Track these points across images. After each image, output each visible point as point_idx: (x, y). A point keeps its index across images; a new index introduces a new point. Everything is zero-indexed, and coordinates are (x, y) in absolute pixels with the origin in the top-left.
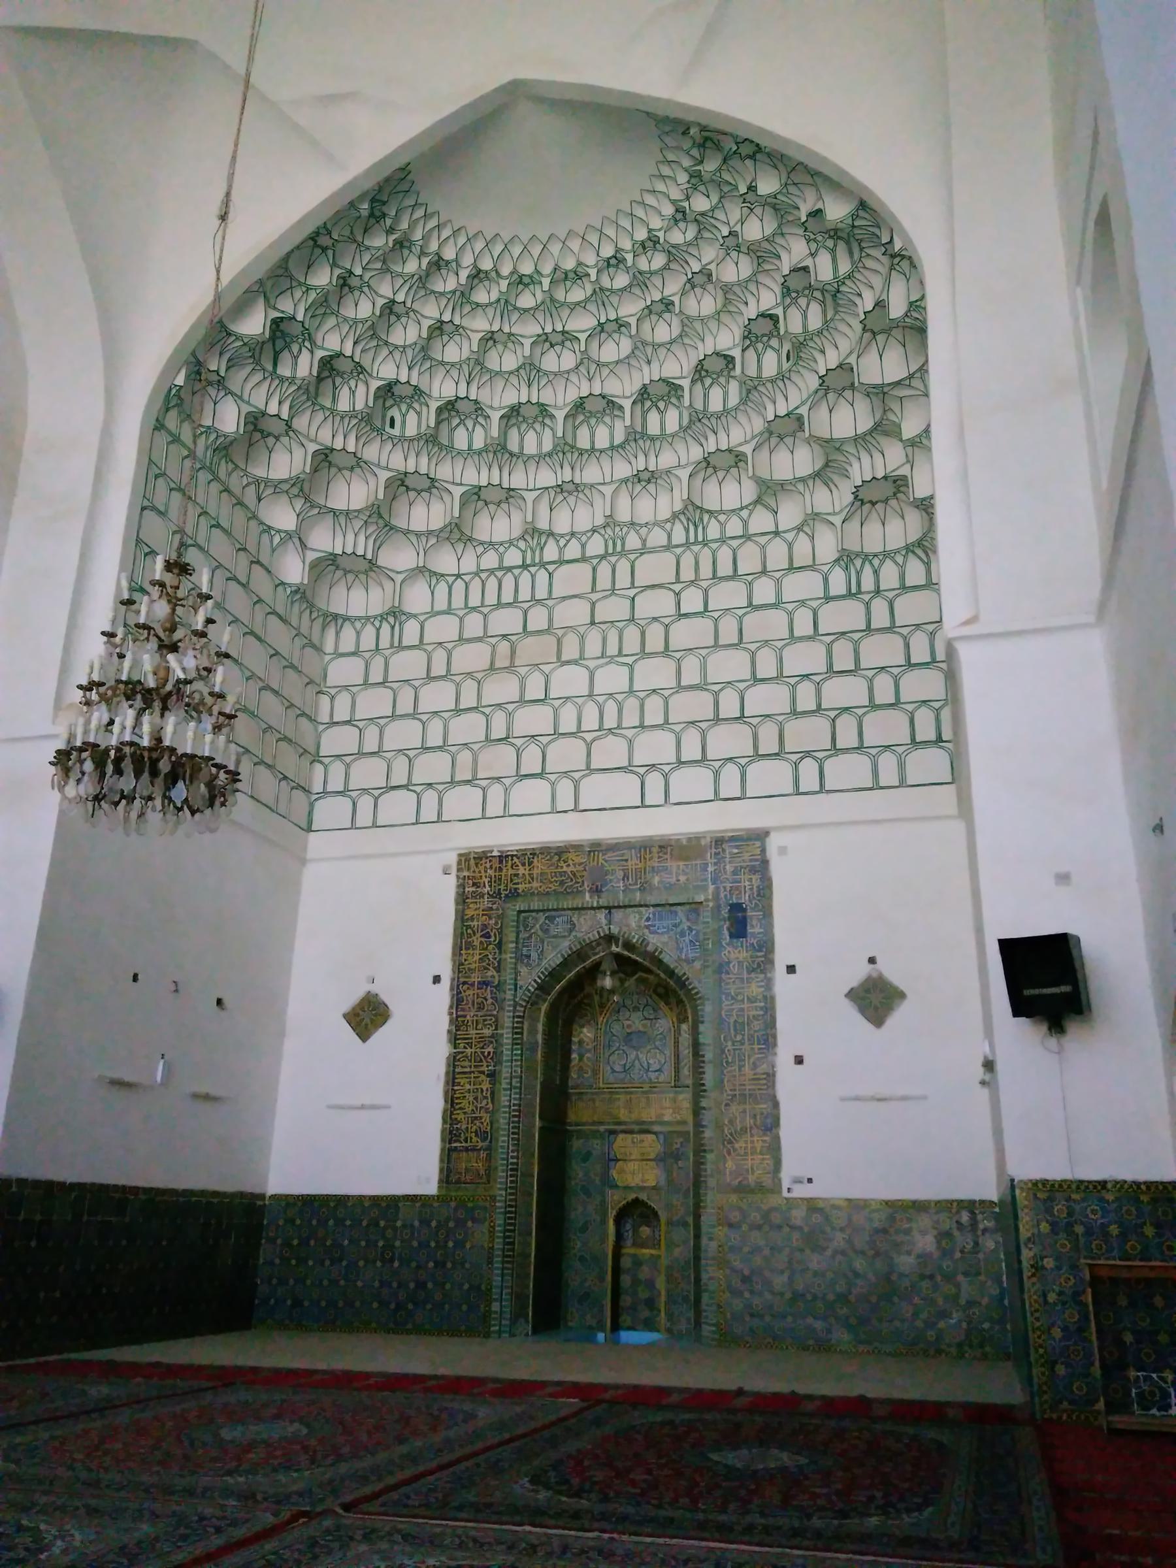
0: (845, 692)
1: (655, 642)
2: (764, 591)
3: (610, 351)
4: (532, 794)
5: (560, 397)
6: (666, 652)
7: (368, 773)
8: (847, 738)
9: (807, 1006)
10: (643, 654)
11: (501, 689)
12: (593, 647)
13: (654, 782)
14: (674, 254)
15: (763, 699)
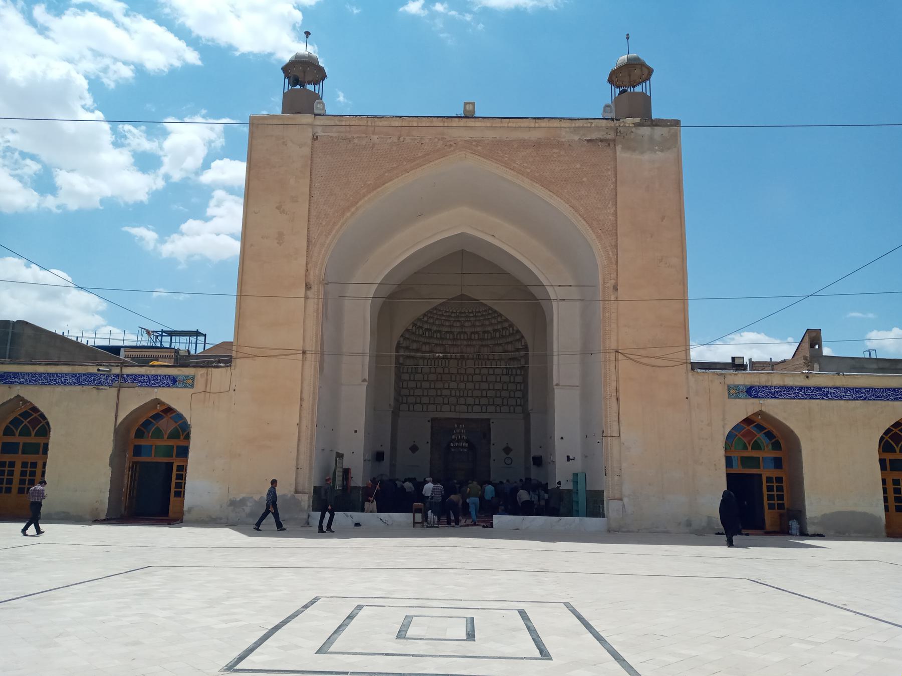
0: (504, 394)
1: (470, 379)
2: (491, 372)
3: (467, 324)
4: (446, 408)
5: (456, 330)
6: (472, 381)
7: (411, 400)
8: (505, 403)
9: (496, 452)
10: (468, 381)
11: (439, 385)
12: (458, 379)
13: (470, 408)
14: (483, 315)
15: (490, 393)
